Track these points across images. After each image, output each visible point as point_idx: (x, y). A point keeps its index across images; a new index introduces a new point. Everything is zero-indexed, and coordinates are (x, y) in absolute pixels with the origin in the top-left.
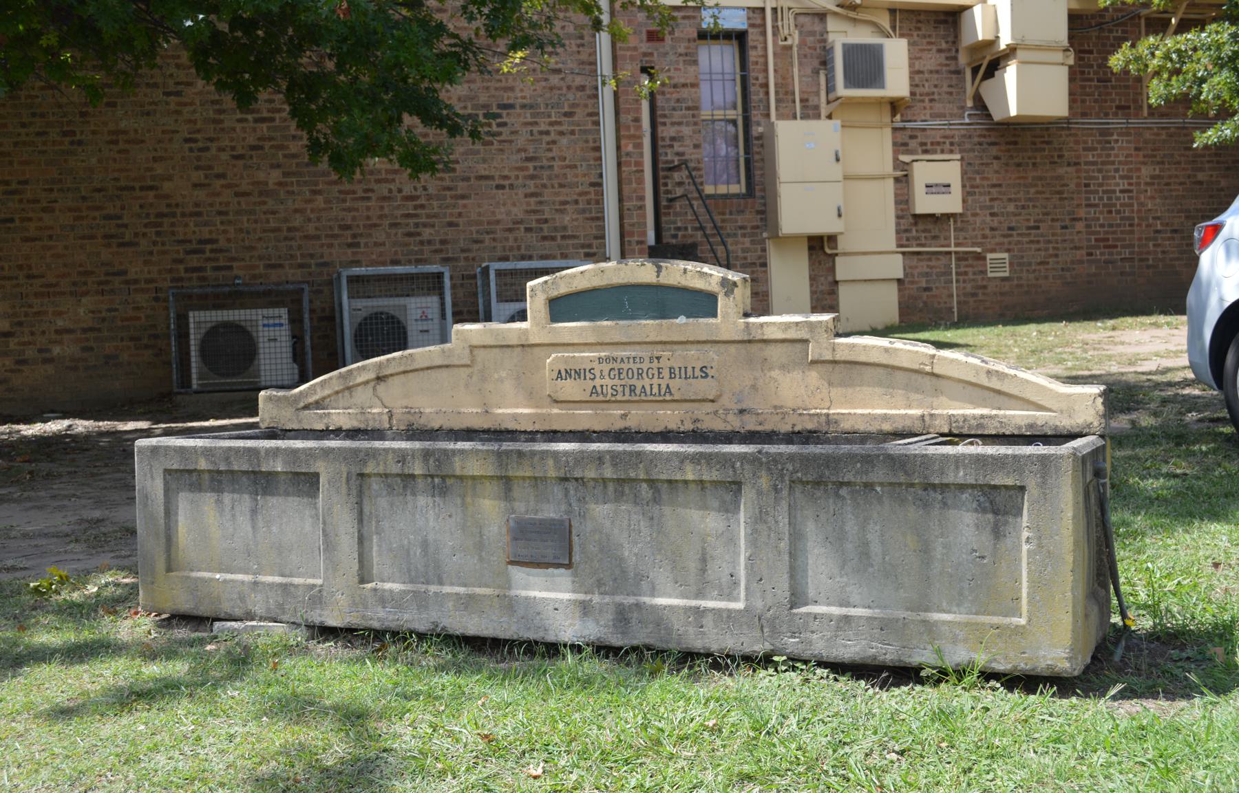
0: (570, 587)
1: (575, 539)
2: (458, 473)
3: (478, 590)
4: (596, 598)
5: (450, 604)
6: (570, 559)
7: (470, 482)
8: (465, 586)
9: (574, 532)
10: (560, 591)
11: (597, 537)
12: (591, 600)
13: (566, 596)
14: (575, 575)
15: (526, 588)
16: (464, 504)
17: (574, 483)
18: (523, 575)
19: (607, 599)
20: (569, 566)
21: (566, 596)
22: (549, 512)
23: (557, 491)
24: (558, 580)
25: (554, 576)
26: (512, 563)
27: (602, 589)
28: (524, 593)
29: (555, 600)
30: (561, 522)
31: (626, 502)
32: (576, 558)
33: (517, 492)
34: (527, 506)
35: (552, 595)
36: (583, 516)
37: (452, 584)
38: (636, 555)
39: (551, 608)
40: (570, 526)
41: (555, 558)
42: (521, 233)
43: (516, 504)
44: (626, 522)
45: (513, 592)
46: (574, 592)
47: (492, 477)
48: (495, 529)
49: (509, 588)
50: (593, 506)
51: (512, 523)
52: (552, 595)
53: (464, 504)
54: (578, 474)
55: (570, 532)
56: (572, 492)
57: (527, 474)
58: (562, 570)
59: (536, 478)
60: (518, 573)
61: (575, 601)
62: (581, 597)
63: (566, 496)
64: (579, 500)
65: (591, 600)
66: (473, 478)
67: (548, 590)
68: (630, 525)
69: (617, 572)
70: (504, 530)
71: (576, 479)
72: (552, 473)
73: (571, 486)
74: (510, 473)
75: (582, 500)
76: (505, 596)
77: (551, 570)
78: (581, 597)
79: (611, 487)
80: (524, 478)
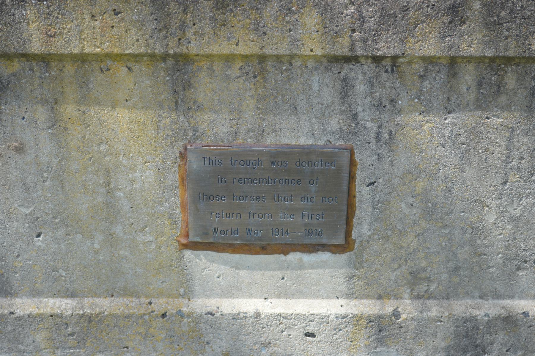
0: (343, 287)
1: (362, 191)
2: (36, 46)
3: (105, 305)
4: (408, 309)
5: (40, 337)
6: (348, 234)
7: (70, 69)
8: (73, 295)
9: (360, 176)
10: (316, 296)
11: (420, 186)
12: (396, 314)
13: (332, 307)
14: (358, 264)
15: (228, 292)
16: (55, 121)
17: (369, 67)
18: (224, 269)
19: (434, 310)
20: (345, 247)
21: (332, 307)
22: (296, 133)
23: (322, 87)
24: (311, 274)
25: (301, 266)
26: (194, 246)
27: (422, 288)
28: (229, 306)
29: (310, 319)
30: (328, 156)
31: (507, 107)
32: (362, 229)
33: (205, 88)
34: (230, 120)
35: (300, 307)
36: (387, 141)
37: (35, 293)
38: (515, 220)
39: (296, 333)
40: (353, 163)
41: (309, 233)
42: (219, 69)
43: (205, 120)
44: (499, 152)
45: (201, 304)
46: (350, 295)
47: (136, 57)
48: (150, 175)
49: (188, 295)
50: (416, 118)
51: (194, 163)
52: (300, 307)
53: (55, 121)
54: (386, 47)
55: (352, 178)
56: (361, 88)
57: (243, 50)
58: (325, 256)
59: (262, 59)
60: (207, 266)
61: (357, 319)
62: (368, 307)
63: (344, 96)
64: (379, 106)
65: (396, 314)
66: (82, 59)
67: (285, 294)
68: (508, 159)
69: (462, 254)
70: (173, 177)
71: (377, 60)
72: (314, 46)
73: (359, 77)
74: (193, 48)
75: (386, 106)
76: (181, 315)
77: (294, 257)
78: (368, 307)
79: (468, 76)
80: (229, 59)
